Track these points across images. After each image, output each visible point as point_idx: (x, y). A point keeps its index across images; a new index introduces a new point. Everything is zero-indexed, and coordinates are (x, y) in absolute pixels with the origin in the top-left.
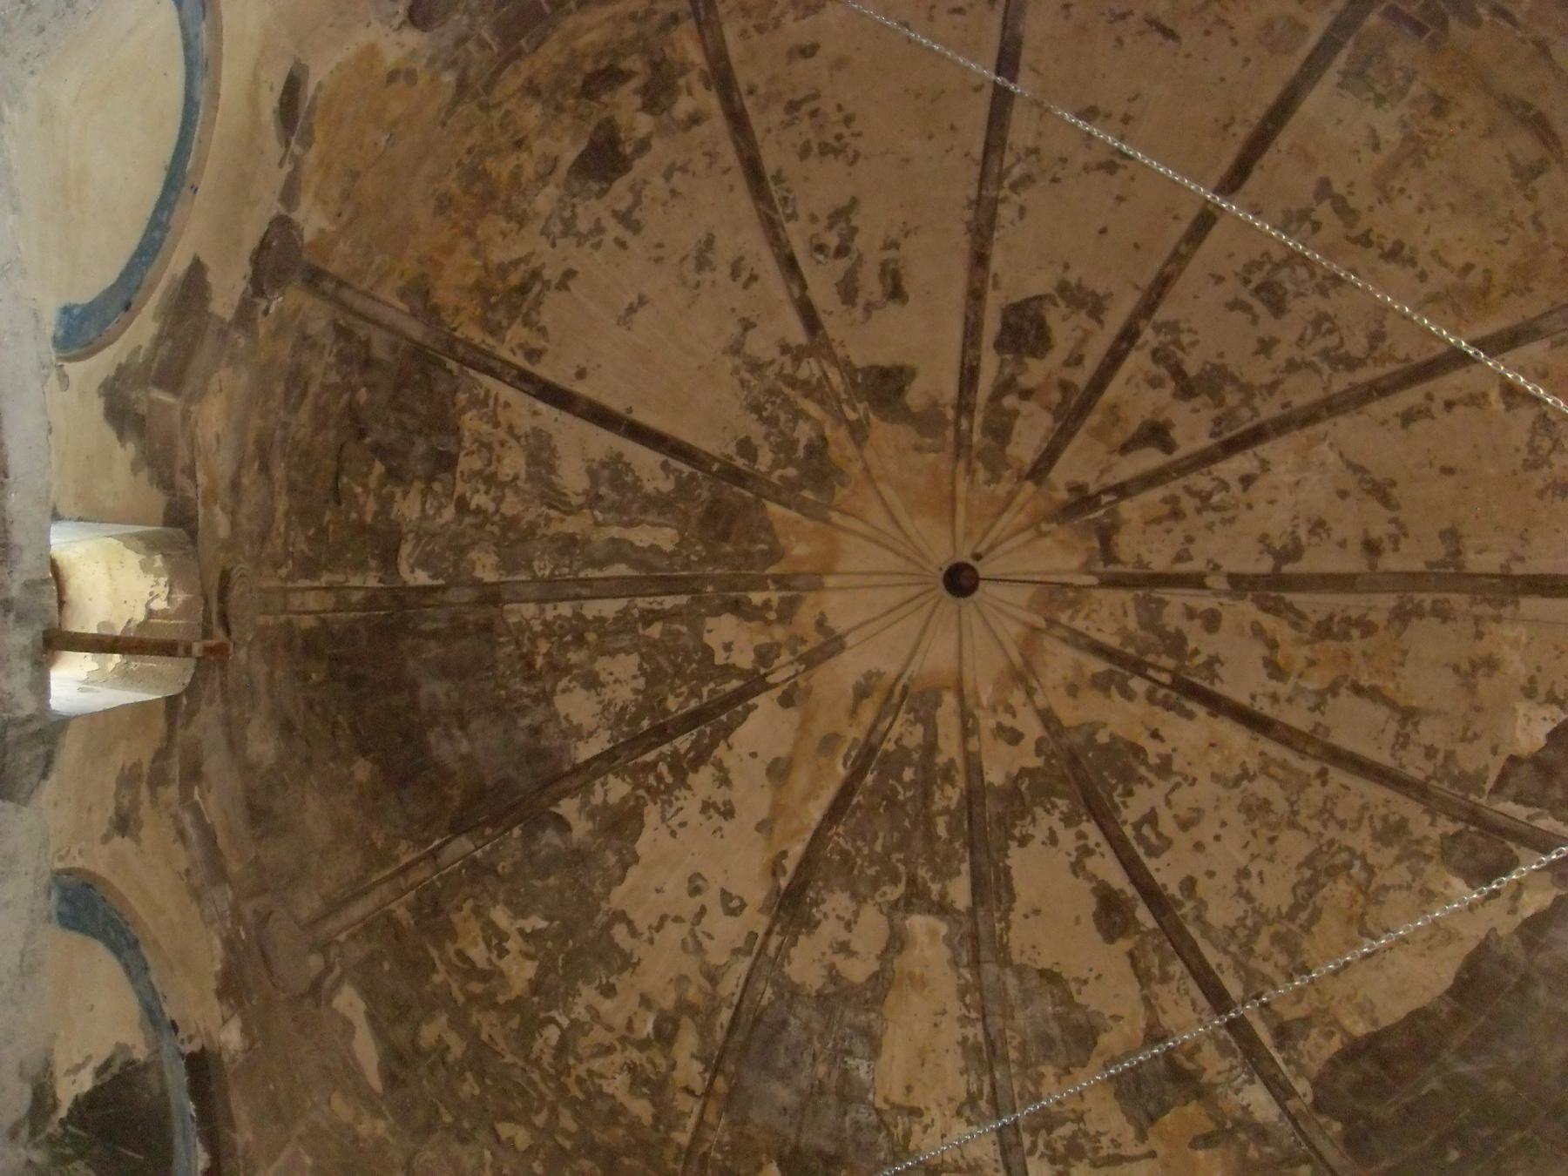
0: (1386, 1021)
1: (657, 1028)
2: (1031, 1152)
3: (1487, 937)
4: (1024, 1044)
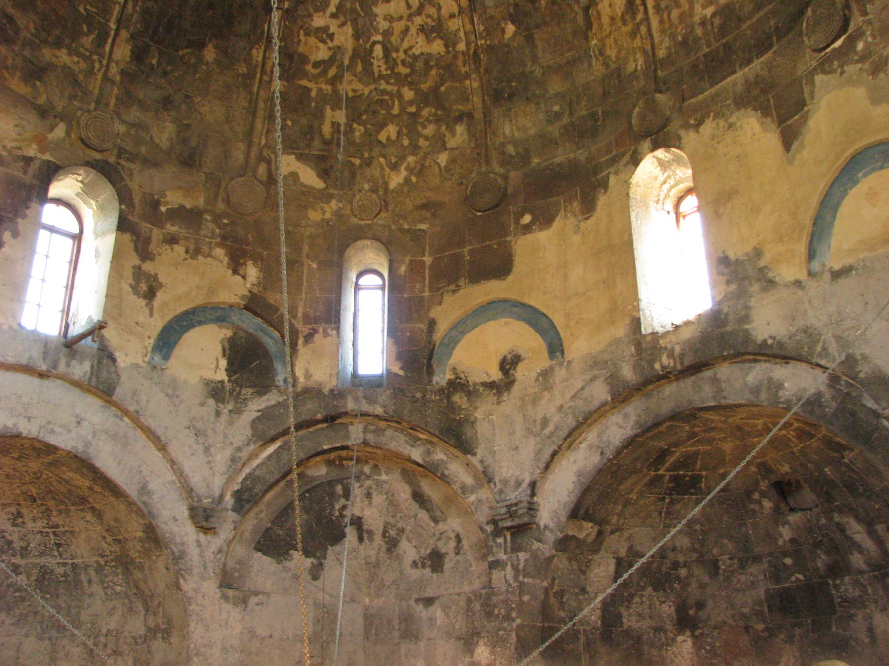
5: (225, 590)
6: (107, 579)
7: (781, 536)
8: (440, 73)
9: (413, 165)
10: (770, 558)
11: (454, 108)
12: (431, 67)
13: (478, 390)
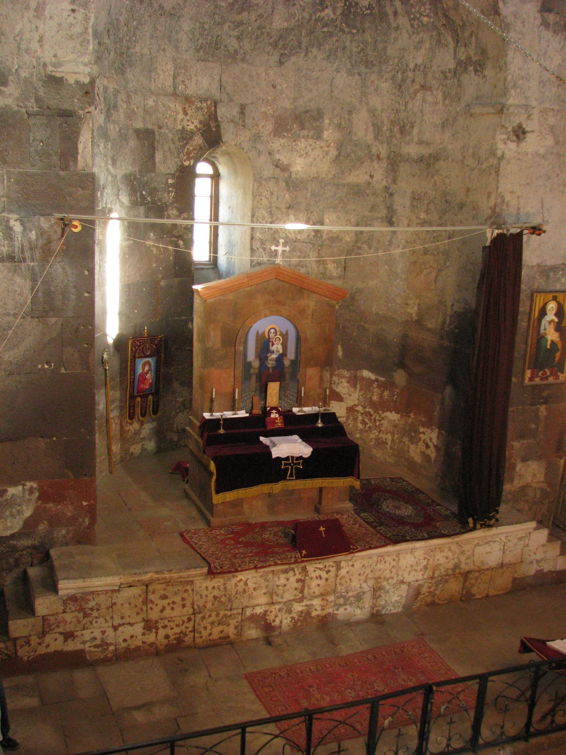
5: (545, 15)
6: (413, 10)
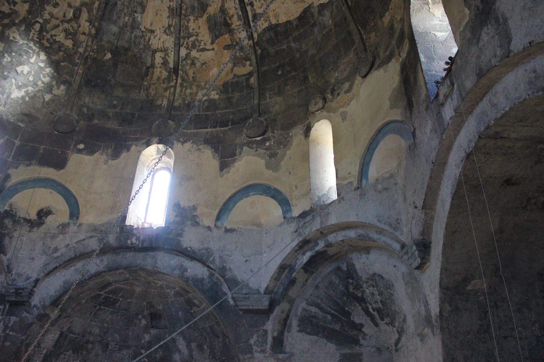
0: (281, 22)
1: (74, 14)
2: (182, 46)
3: (311, 4)
4: (187, 8)
7: (144, 338)
8: (64, 56)
9: (30, 92)
10: (135, 348)
11: (64, 76)
12: (61, 51)
13: (20, 221)
